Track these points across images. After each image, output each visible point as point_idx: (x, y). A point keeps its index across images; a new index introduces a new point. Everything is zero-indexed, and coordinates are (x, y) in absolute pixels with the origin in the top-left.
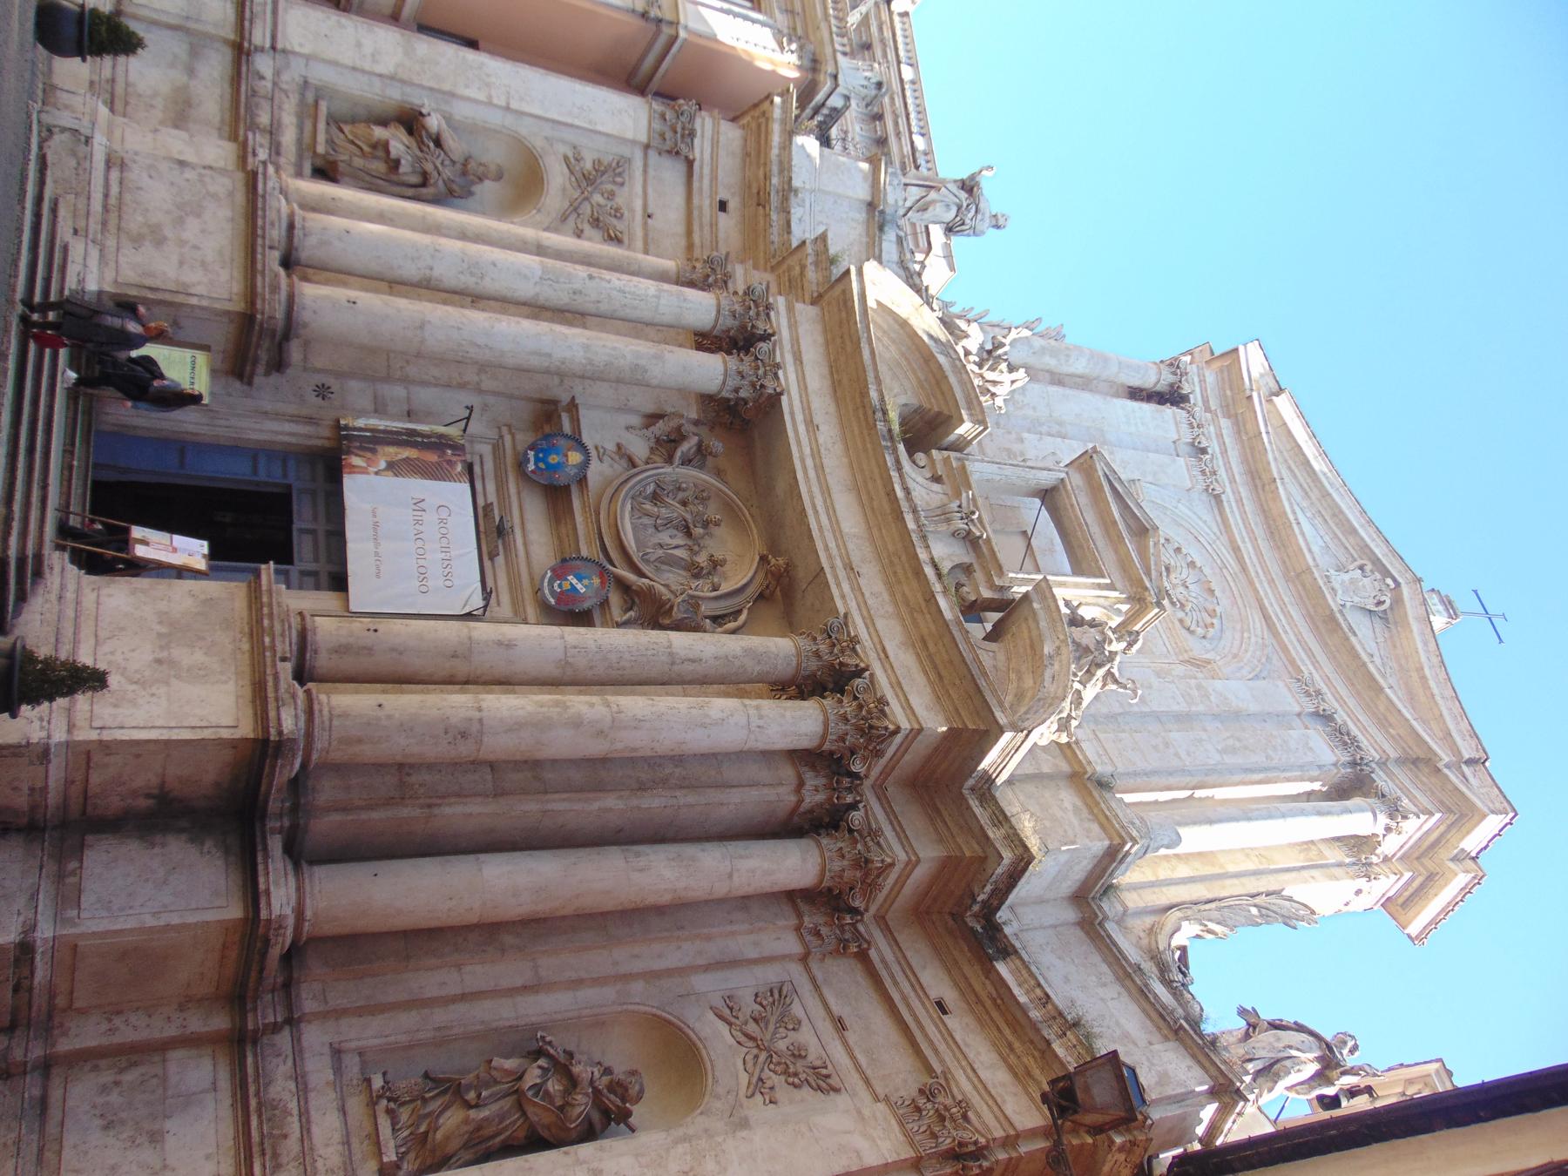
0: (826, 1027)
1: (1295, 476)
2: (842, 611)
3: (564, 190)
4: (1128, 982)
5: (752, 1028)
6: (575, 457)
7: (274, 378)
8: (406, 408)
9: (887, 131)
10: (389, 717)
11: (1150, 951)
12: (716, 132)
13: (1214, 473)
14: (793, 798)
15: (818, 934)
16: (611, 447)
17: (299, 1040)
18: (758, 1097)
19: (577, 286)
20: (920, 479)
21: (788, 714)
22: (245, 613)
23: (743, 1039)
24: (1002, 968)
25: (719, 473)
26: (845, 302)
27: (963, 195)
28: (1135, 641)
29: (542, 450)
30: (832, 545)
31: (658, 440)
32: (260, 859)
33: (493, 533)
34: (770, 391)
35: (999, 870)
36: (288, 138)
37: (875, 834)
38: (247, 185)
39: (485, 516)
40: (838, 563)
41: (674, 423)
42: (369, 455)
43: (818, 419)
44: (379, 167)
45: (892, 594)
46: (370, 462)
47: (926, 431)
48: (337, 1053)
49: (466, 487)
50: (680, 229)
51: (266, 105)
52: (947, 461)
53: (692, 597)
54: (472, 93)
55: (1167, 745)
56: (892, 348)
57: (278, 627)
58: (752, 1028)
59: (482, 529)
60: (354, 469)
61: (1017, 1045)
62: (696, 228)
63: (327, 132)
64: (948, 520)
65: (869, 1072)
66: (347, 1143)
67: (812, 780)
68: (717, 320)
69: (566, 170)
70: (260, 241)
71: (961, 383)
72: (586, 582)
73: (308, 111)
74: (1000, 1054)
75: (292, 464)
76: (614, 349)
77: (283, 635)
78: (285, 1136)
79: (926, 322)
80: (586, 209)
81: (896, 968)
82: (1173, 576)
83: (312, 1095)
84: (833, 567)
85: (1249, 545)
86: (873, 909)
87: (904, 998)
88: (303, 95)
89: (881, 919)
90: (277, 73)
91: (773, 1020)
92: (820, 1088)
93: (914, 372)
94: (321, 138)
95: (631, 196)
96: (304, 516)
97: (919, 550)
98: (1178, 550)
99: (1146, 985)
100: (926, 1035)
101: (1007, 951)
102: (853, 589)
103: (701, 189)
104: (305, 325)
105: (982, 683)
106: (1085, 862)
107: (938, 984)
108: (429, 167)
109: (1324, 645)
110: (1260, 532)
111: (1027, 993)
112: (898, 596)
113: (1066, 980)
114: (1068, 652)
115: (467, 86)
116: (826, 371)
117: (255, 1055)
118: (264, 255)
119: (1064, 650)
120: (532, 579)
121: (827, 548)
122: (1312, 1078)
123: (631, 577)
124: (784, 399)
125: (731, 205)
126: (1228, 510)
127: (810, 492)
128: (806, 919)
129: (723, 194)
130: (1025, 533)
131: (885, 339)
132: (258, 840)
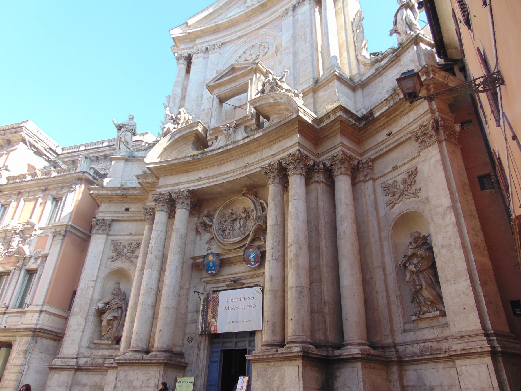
0: (396, 172)
1: (215, 18)
2: (260, 169)
3: (122, 262)
4: (381, 73)
5: (396, 197)
6: (211, 257)
7: (186, 356)
8: (195, 313)
9: (101, 155)
10: (295, 317)
11: (371, 66)
12: (103, 212)
13: (214, 45)
14: (322, 184)
15: (366, 175)
16: (207, 246)
17: (401, 343)
18: (419, 194)
19: (154, 257)
20: (216, 144)
21: (294, 186)
22: (262, 364)
23: (400, 200)
24: (377, 115)
25: (215, 210)
26: (158, 169)
27: (122, 130)
28: (269, 72)
29: (208, 268)
30: (238, 172)
31: (205, 230)
32: (342, 357)
33: (236, 284)
34: (188, 193)
35: (345, 116)
36: (107, 353)
37: (333, 157)
38: (122, 366)
39: (230, 286)
40: (244, 170)
41: (199, 225)
42: (210, 325)
43: (197, 177)
44: (116, 323)
45: (254, 152)
46: (213, 324)
47: (201, 142)
48: (405, 331)
49: (221, 293)
50: (135, 224)
51: (96, 360)
52: (210, 135)
53: (256, 218)
54: (91, 293)
55: (304, 61)
56: (173, 153)
57: (267, 353)
58: (396, 197)
59: (234, 287)
60: (215, 329)
61: (401, 110)
62: (135, 218)
63: (104, 340)
64: (230, 134)
65: (411, 158)
66: (433, 327)
67: (316, 178)
68: (165, 211)
69: (116, 261)
70: (140, 361)
71: (184, 130)
72: (251, 253)
73: (98, 346)
74: (405, 115)
75: (215, 350)
76: (174, 245)
77: (269, 352)
78: (431, 347)
79: (165, 142)
80: (129, 255)
81: (377, 150)
82: (248, 59)
83: (418, 339)
84: (246, 172)
85: (238, 33)
86: (358, 157)
87: (387, 147)
88: (92, 348)
89: (361, 155)
90: (85, 357)
91: (394, 190)
92: (416, 174)
93: (181, 146)
94: (106, 342)
95: (125, 240)
96: (231, 345)
97: (240, 144)
98: (240, 57)
99: (382, 67)
100: (399, 139)
101: (371, 113)
102: (253, 166)
103: (122, 217)
104: (168, 346)
105: (283, 122)
106: (342, 88)
107: (382, 136)
108: (116, 306)
109: (270, 8)
110: (233, 30)
111: (384, 106)
112: (255, 150)
113: (381, 93)
114: (273, 94)
115: (89, 294)
116: (181, 175)
117: (405, 357)
118: (145, 360)
119: (272, 95)
120: (251, 271)
121: (239, 174)
122: (412, 11)
123: (250, 238)
124: (190, 189)
125: (127, 207)
126: (226, 40)
127: (221, 180)
128: (361, 179)
129: (123, 209)
130: (234, 108)
131: (170, 155)
132: (335, 358)
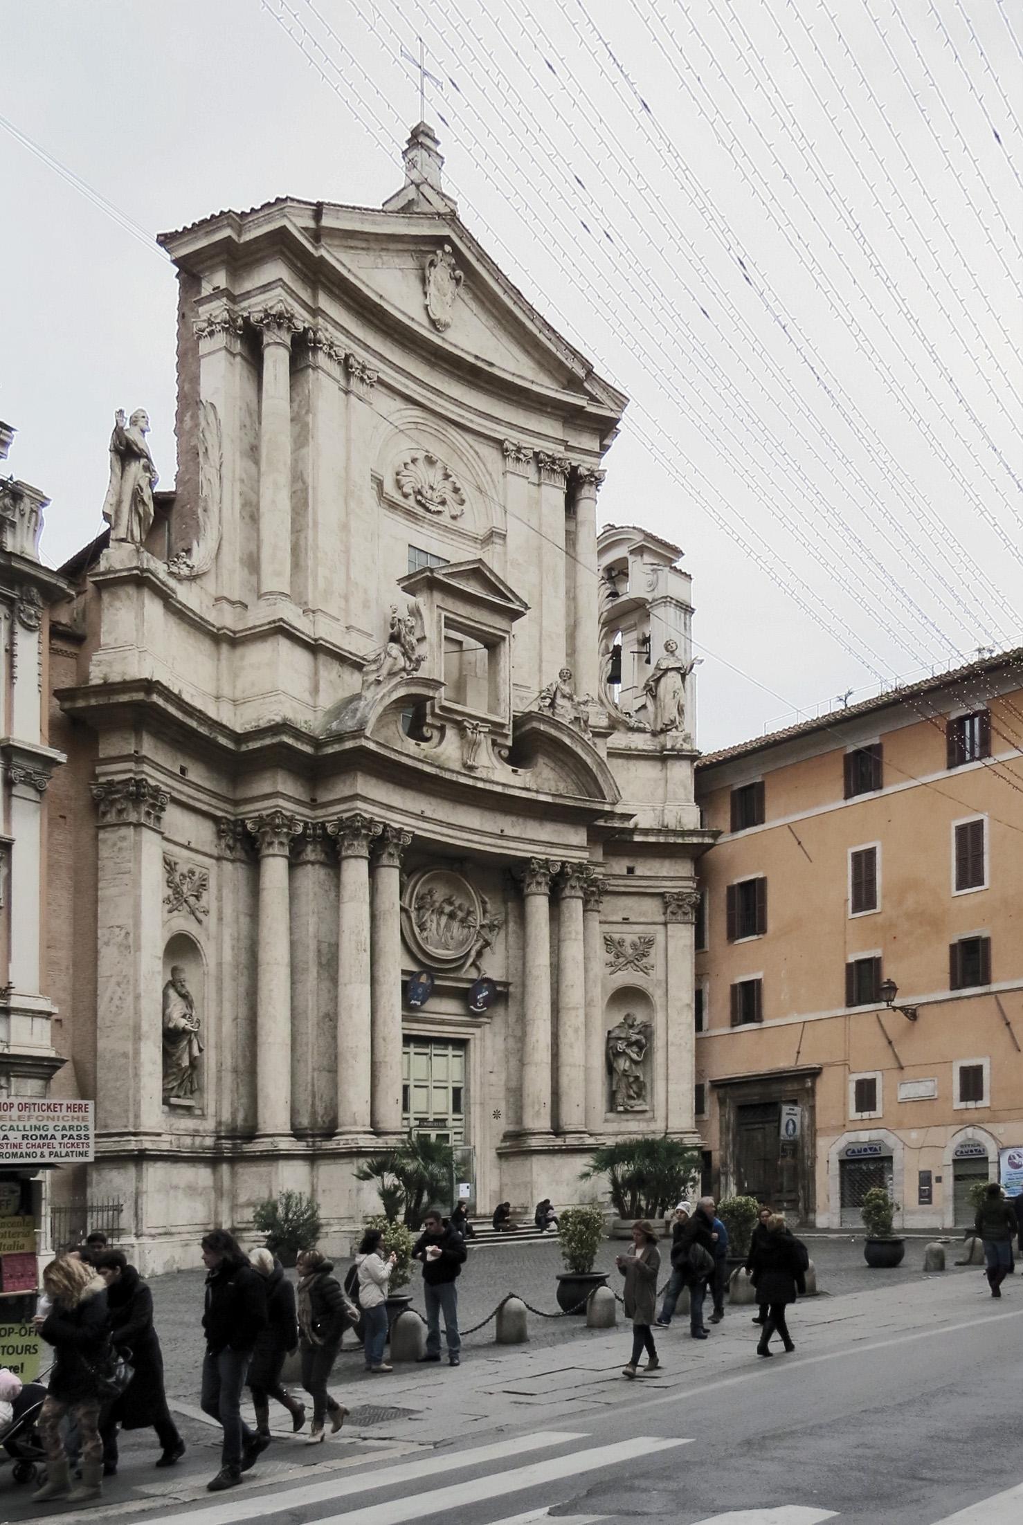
0: (626, 928)
3: (186, 918)
5: (621, 960)
40: (499, 842)
124: (418, 832)
